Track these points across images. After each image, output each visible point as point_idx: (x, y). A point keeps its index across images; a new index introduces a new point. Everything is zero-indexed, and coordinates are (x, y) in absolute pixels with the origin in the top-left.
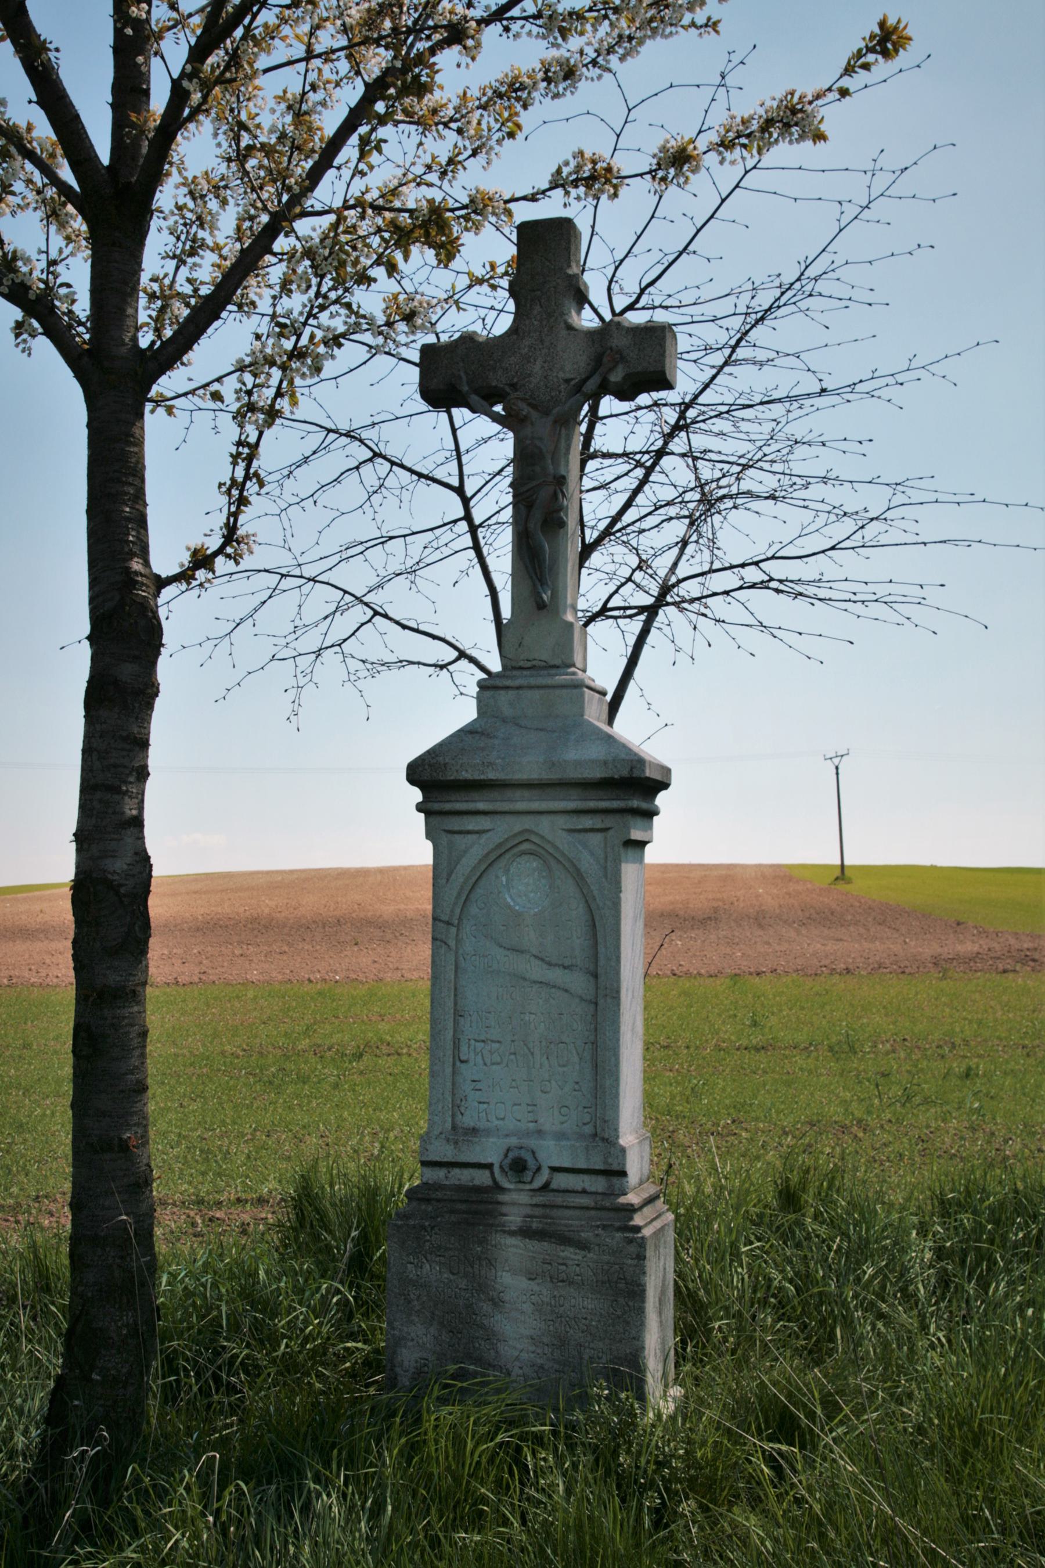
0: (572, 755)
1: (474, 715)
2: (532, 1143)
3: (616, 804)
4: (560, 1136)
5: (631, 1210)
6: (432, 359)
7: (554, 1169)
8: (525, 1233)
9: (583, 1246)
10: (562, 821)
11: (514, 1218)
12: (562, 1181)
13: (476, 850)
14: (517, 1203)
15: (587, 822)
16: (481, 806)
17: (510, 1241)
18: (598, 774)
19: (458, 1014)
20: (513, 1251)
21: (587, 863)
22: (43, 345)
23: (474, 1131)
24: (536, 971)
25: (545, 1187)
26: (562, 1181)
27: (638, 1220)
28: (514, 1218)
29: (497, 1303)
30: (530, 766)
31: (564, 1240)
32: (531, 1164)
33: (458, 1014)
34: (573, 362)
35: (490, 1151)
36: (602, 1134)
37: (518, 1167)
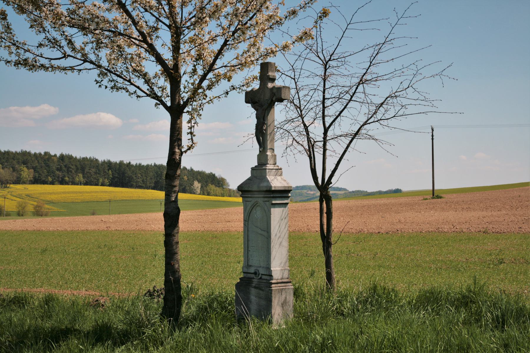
0: (262, 185)
1: (250, 175)
2: (258, 269)
3: (269, 196)
4: (263, 267)
5: (272, 284)
6: (247, 93)
7: (262, 274)
8: (255, 287)
9: (263, 290)
10: (262, 199)
11: (254, 285)
12: (264, 277)
13: (250, 204)
14: (255, 281)
15: (266, 199)
16: (250, 196)
17: (253, 289)
18: (265, 189)
19: (248, 241)
20: (253, 291)
21: (266, 208)
22: (161, 107)
23: (251, 266)
24: (260, 231)
25: (261, 278)
26: (264, 277)
27: (273, 286)
28: (254, 285)
29: (251, 302)
30: (255, 188)
31: (260, 289)
32: (258, 273)
33: (248, 241)
34: (268, 95)
35: (252, 270)
36: (268, 268)
37: (255, 273)
